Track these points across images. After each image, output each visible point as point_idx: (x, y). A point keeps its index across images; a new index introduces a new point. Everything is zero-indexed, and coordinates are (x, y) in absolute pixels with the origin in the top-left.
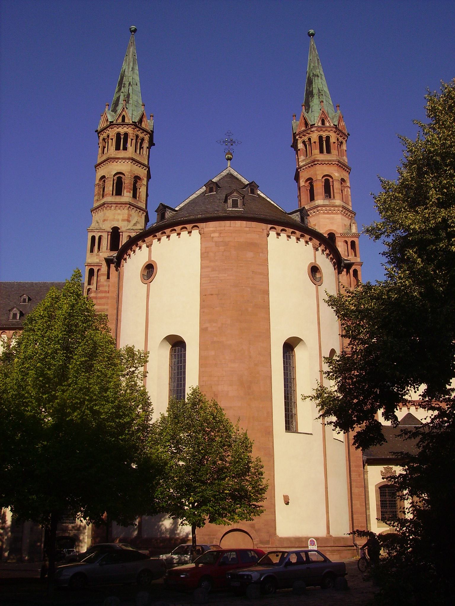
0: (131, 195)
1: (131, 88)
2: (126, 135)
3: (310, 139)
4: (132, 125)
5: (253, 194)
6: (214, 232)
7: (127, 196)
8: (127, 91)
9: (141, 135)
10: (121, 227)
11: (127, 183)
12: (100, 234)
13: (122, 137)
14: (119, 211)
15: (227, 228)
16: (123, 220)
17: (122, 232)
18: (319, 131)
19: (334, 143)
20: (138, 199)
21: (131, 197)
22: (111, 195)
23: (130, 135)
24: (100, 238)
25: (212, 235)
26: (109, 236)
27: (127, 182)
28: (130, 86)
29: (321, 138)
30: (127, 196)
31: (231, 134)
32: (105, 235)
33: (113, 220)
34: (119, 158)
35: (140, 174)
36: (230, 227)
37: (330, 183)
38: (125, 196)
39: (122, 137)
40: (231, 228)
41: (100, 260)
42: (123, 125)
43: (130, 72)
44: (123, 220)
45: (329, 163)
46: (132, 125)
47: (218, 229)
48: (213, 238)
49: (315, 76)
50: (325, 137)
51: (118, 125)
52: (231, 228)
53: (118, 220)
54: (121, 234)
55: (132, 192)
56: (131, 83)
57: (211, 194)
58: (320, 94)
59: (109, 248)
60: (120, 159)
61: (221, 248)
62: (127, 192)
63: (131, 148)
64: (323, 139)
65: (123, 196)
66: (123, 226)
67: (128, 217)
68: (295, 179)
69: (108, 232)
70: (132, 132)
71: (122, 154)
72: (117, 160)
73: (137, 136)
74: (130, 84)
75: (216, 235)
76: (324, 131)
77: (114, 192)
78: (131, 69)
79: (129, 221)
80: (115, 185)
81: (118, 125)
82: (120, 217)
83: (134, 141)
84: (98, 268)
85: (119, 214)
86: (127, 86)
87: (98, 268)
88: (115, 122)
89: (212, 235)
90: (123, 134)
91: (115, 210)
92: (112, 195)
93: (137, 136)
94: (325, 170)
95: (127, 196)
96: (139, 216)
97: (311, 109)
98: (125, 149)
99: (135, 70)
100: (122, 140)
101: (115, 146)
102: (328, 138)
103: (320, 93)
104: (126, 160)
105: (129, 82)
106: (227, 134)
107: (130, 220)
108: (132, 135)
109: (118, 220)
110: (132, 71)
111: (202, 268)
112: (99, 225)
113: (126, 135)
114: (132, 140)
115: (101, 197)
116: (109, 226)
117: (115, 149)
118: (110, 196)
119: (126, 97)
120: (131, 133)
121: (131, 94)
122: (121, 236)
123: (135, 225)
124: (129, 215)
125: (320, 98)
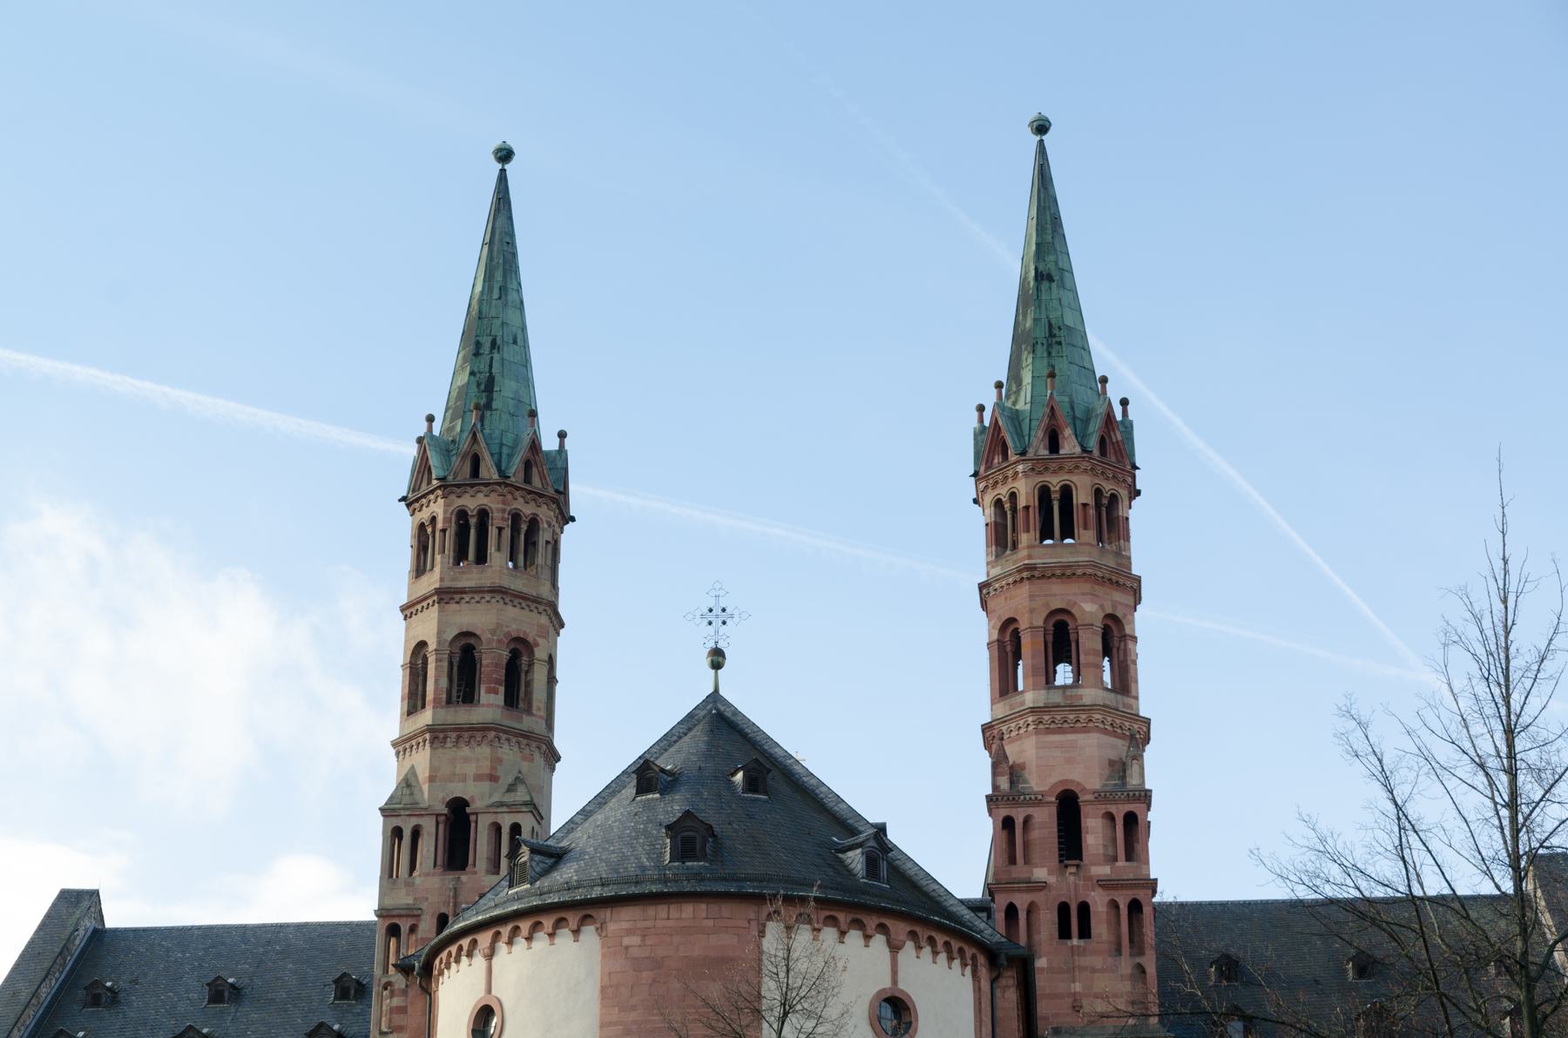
0: (500, 699)
1: (496, 356)
2: (483, 514)
3: (1013, 496)
4: (499, 484)
5: (755, 791)
6: (630, 932)
7: (488, 705)
8: (487, 369)
9: (527, 510)
10: (472, 798)
11: (487, 666)
12: (414, 821)
13: (473, 521)
14: (465, 751)
15: (660, 923)
16: (478, 778)
17: (477, 814)
18: (1040, 473)
19: (1085, 505)
20: (521, 705)
21: (498, 706)
22: (444, 704)
23: (495, 514)
24: (416, 833)
25: (626, 941)
26: (441, 827)
27: (491, 660)
28: (496, 351)
29: (1044, 493)
30: (489, 705)
31: (721, 593)
32: (428, 825)
33: (451, 778)
34: (462, 591)
35: (525, 632)
36: (668, 919)
37: (1069, 633)
38: (483, 705)
39: (473, 521)
40: (671, 923)
41: (415, 899)
42: (472, 486)
43: (494, 302)
44: (478, 778)
45: (1066, 574)
46: (499, 484)
47: (641, 924)
48: (627, 948)
49: (1042, 279)
50: (1057, 488)
51: (458, 486)
52: (671, 923)
53: (464, 779)
54: (472, 818)
55: (502, 689)
56: (499, 341)
57: (648, 800)
58: (1054, 340)
59: (439, 862)
60: (466, 593)
61: (645, 974)
62: (489, 691)
63: (498, 558)
64: (1053, 496)
65: (476, 706)
66: (479, 795)
67: (493, 768)
68: (982, 607)
69: (438, 815)
70: (500, 506)
71: (471, 577)
72: (457, 597)
73: (516, 517)
74: (494, 344)
75: (634, 940)
76: (1055, 472)
77: (454, 693)
78: (496, 295)
79: (493, 778)
80: (455, 669)
81: (458, 486)
82: (471, 769)
83: (507, 533)
84: (410, 922)
85: (466, 760)
86: (487, 352)
87: (410, 922)
88: (450, 478)
89: (626, 941)
90: (475, 513)
91: (455, 749)
92: (449, 702)
93: (516, 517)
94: (1055, 595)
95: (489, 705)
96: (524, 758)
97: (1023, 394)
98: (481, 558)
99: (510, 291)
100: (473, 532)
101: (452, 553)
102: (1066, 492)
103: (1055, 336)
104: (485, 595)
105: (490, 338)
106: (713, 593)
107: (498, 774)
108: (500, 515)
109: (464, 779)
110: (500, 298)
111: (602, 1026)
112: (412, 794)
113: (483, 514)
114: (500, 529)
115: (419, 708)
116: (441, 795)
117: (451, 560)
118: (442, 708)
119: (483, 387)
120: (498, 510)
121: (498, 378)
122: (473, 825)
123: (511, 788)
124: (496, 761)
125: (1053, 354)
